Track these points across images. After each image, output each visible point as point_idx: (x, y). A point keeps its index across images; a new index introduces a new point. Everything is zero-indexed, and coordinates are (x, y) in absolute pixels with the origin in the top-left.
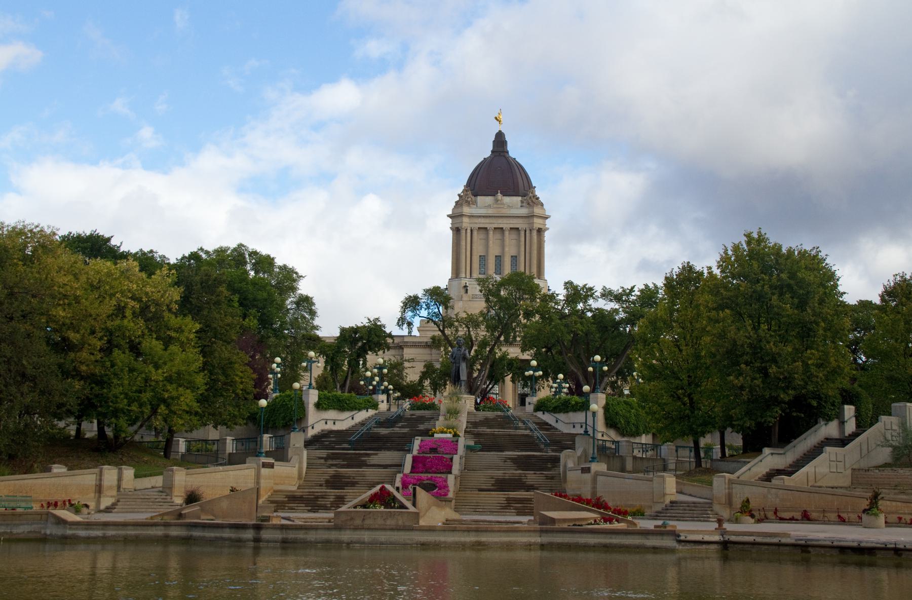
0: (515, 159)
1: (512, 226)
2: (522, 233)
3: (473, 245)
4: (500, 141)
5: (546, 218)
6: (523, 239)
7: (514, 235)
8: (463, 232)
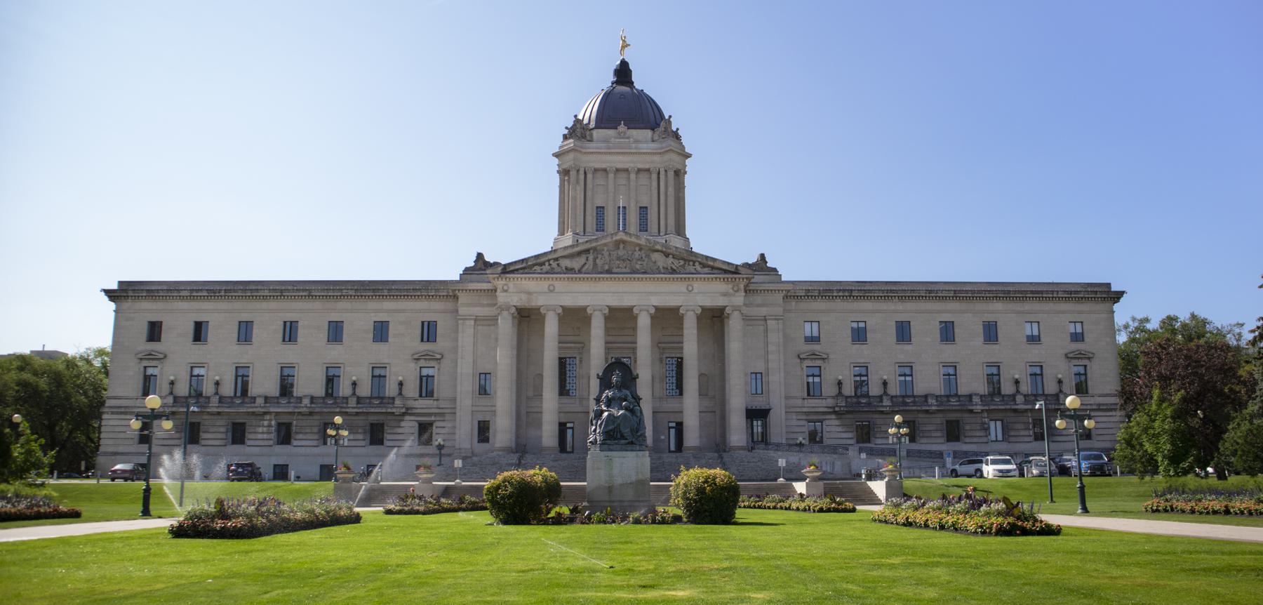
0: (642, 90)
1: (640, 166)
2: (654, 176)
3: (587, 194)
4: (623, 73)
5: (689, 156)
6: (655, 184)
7: (643, 179)
8: (573, 173)
